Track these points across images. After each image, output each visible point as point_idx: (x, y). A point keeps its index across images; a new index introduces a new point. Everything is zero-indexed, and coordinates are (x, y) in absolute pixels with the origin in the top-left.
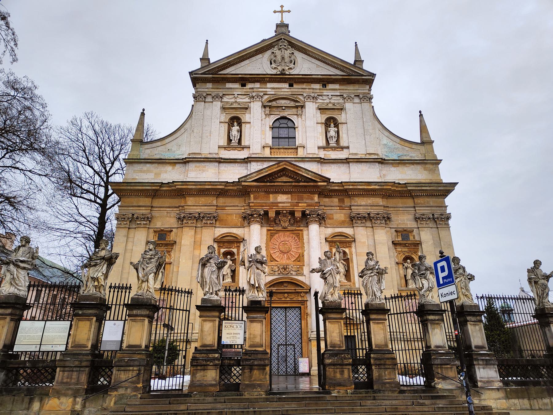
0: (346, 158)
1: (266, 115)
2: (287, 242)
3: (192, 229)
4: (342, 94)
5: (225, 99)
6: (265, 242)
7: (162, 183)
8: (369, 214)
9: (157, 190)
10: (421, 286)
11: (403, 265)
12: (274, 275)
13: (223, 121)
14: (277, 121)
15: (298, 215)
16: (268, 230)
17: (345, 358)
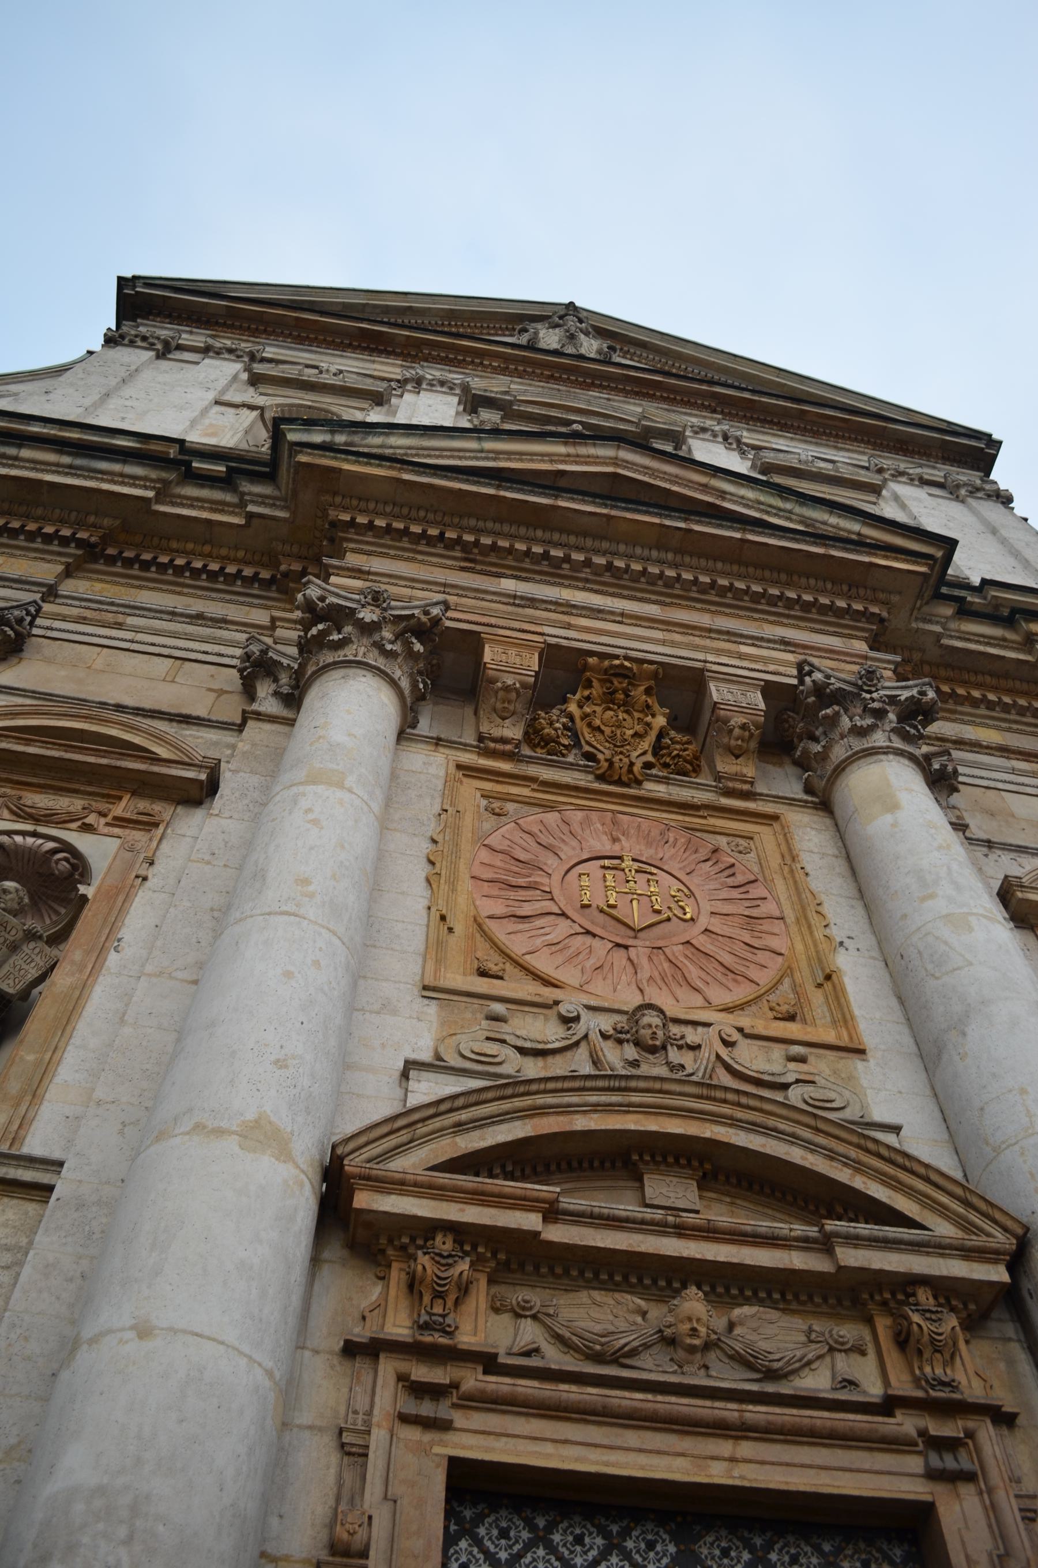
6: (432, 828)
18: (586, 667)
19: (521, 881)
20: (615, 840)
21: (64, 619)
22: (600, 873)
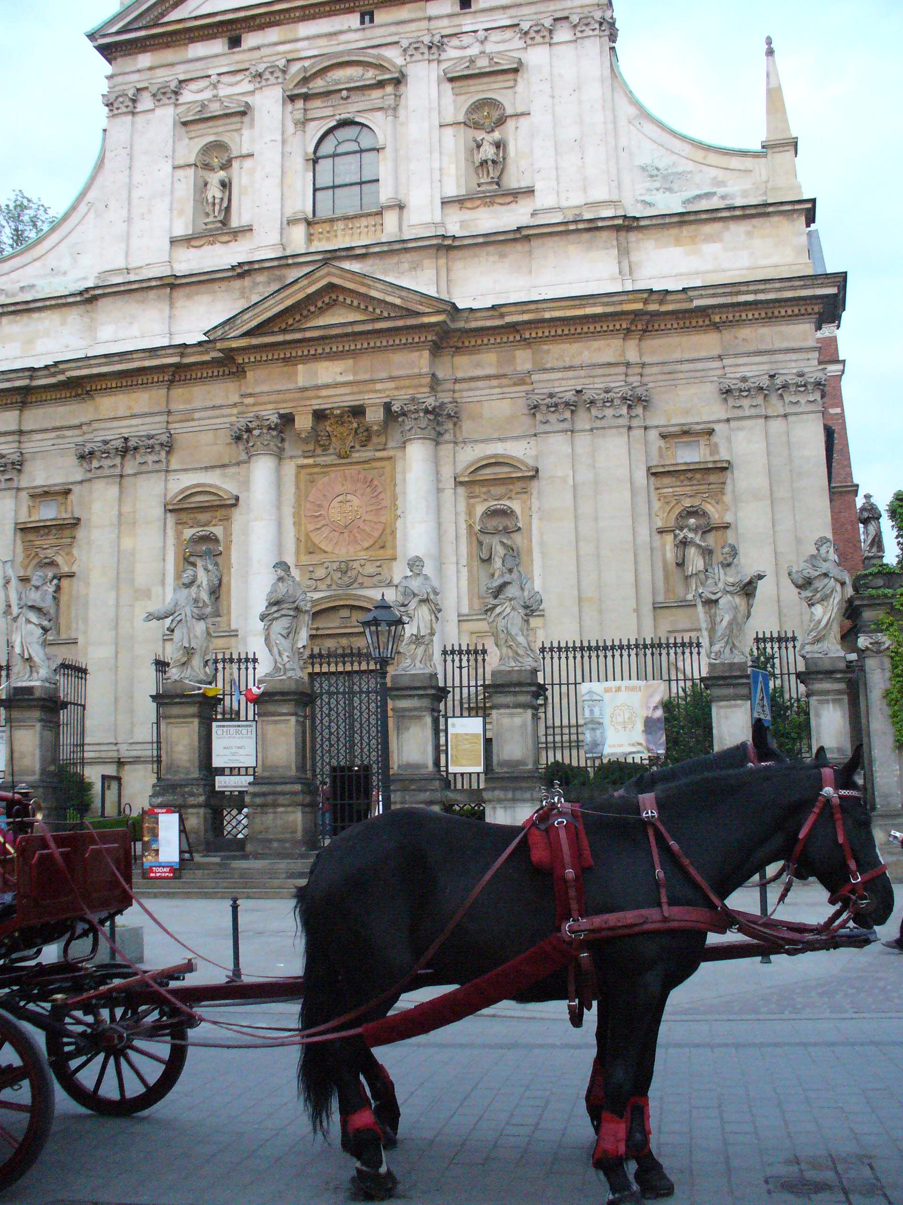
0: (519, 229)
1: (296, 124)
2: (349, 497)
4: (515, 22)
5: (187, 96)
6: (293, 500)
7: (32, 369)
8: (578, 392)
11: (676, 536)
12: (316, 590)
13: (181, 162)
14: (331, 137)
15: (375, 416)
16: (301, 467)
17: (192, 794)
20: (343, 485)
21: (176, 422)
22: (337, 505)
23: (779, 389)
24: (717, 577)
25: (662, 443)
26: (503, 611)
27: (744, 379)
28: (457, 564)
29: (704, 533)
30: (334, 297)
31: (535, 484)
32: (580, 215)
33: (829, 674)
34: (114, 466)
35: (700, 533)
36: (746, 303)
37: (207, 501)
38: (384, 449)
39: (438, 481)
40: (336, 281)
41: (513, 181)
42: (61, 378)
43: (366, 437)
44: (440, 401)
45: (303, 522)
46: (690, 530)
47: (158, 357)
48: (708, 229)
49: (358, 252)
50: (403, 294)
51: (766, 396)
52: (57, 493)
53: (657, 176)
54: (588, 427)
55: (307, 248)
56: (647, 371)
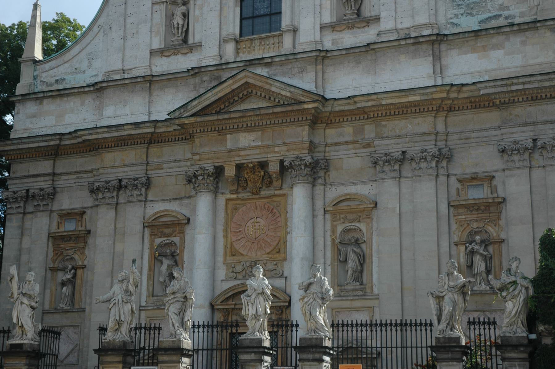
0: (368, 45)
2: (258, 220)
3: (111, 208)
8: (404, 152)
9: (58, 146)
10: (248, 313)
11: (466, 248)
15: (273, 168)
16: (228, 200)
18: (245, 167)
19: (238, 230)
21: (152, 170)
23: (540, 148)
24: (443, 282)
25: (459, 185)
26: (309, 300)
27: (515, 142)
28: (325, 264)
29: (486, 246)
30: (250, 91)
31: (375, 212)
32: (409, 34)
33: (515, 347)
34: (113, 197)
35: (483, 246)
36: (517, 91)
37: (171, 221)
38: (281, 189)
39: (314, 210)
40: (251, 81)
41: (366, 12)
42: (80, 140)
43: (267, 180)
44: (315, 158)
45: (229, 236)
46: (476, 244)
47: (140, 128)
48: (495, 40)
49: (266, 61)
50: (292, 89)
51: (530, 153)
52: (76, 214)
53: (462, 5)
54: (410, 175)
55: (235, 58)
56: (450, 137)
